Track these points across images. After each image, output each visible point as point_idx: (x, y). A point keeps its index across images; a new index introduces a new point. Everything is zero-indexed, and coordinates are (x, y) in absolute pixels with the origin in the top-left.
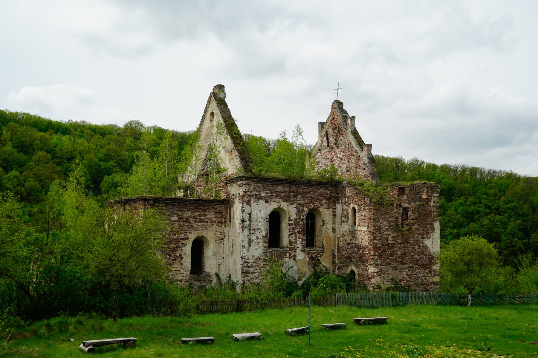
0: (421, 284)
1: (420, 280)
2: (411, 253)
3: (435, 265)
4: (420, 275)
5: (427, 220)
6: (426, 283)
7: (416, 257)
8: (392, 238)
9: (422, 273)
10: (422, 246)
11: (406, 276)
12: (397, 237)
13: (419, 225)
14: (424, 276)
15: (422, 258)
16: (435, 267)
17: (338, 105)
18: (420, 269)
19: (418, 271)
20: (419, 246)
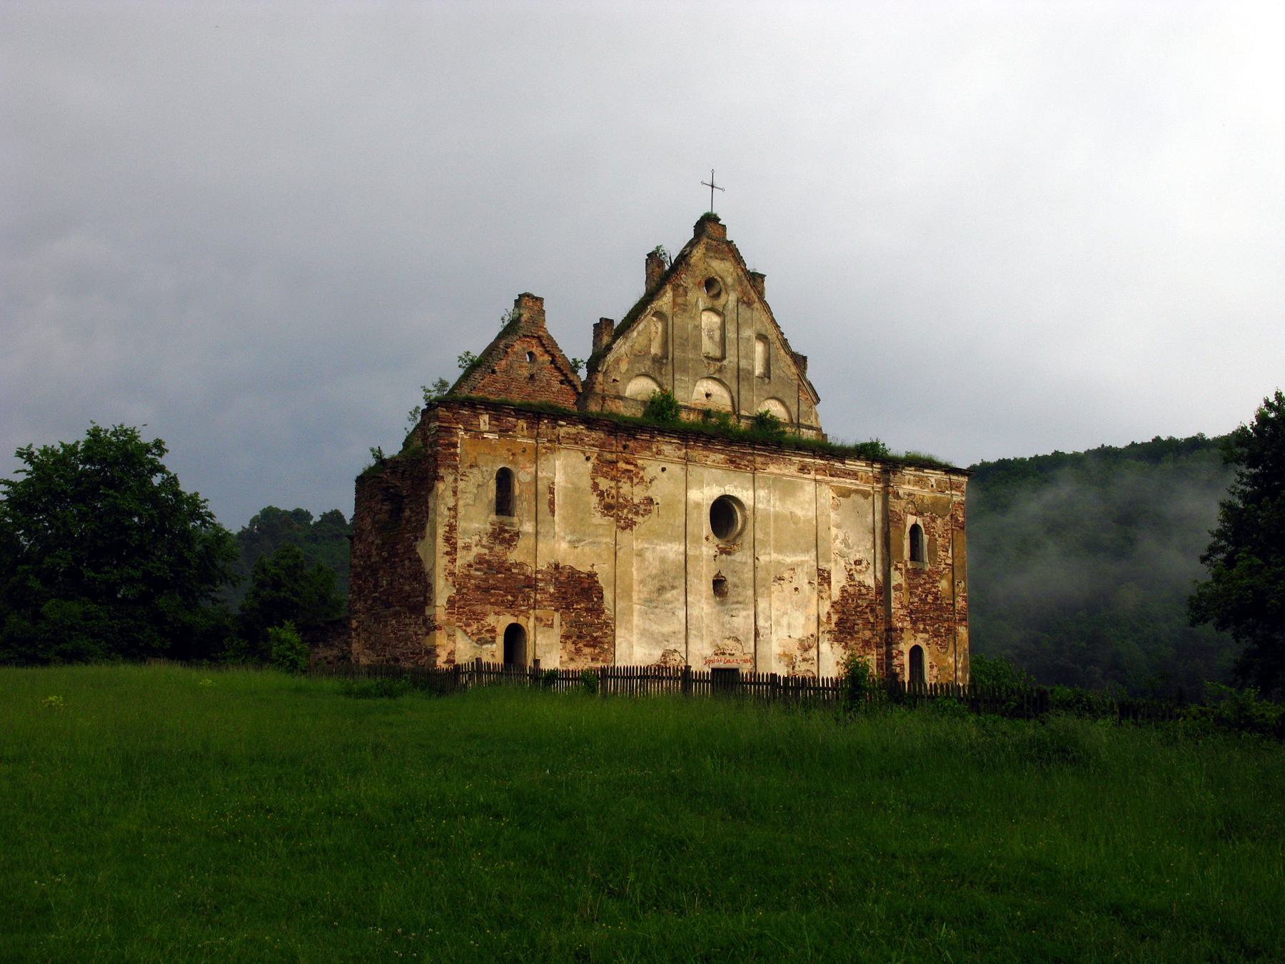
0: (411, 653)
1: (409, 643)
2: (401, 580)
3: (429, 605)
4: (411, 630)
5: (423, 493)
6: (417, 651)
7: (407, 588)
8: (376, 549)
9: (413, 626)
10: (415, 561)
11: (392, 635)
12: (383, 544)
13: (411, 509)
14: (416, 634)
15: (414, 589)
16: (428, 612)
17: (708, 226)
18: (410, 617)
19: (407, 621)
20: (410, 559)
